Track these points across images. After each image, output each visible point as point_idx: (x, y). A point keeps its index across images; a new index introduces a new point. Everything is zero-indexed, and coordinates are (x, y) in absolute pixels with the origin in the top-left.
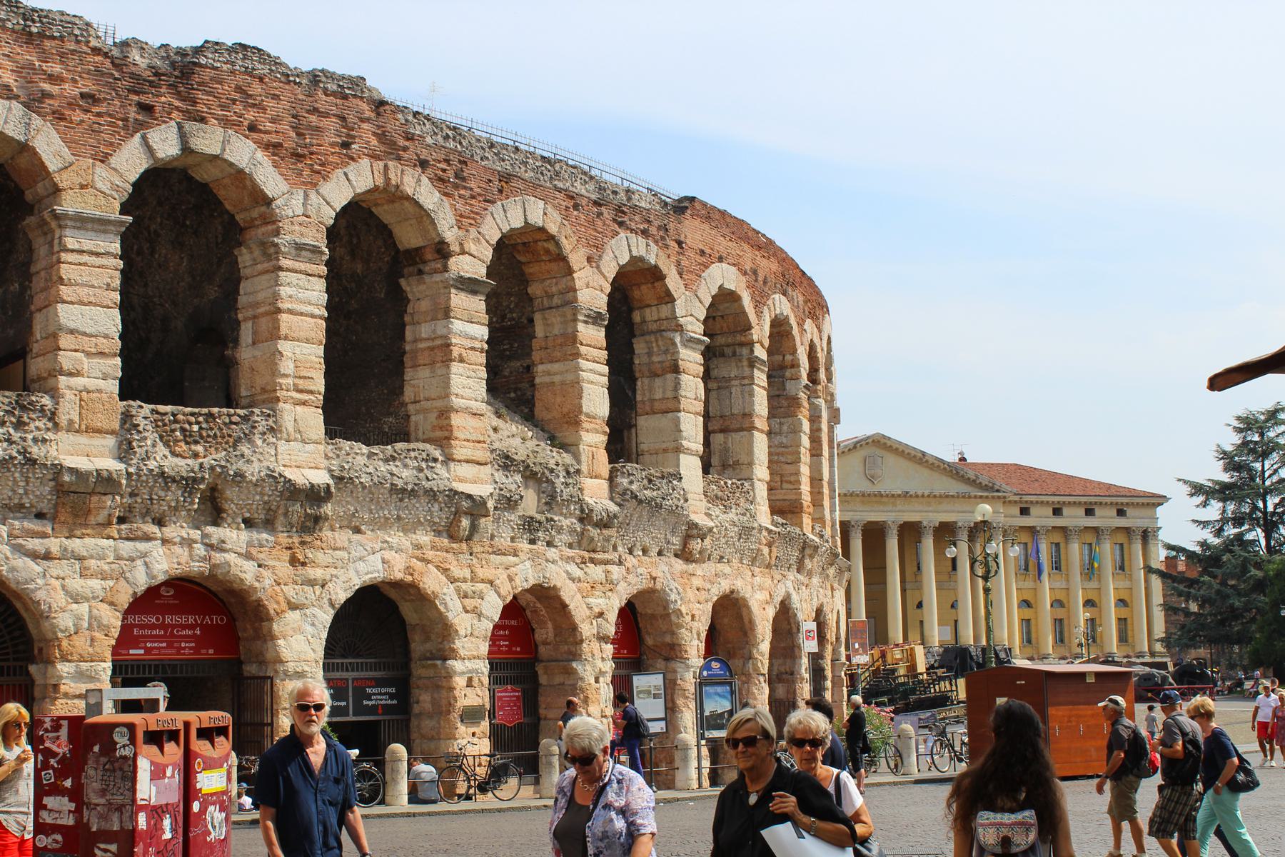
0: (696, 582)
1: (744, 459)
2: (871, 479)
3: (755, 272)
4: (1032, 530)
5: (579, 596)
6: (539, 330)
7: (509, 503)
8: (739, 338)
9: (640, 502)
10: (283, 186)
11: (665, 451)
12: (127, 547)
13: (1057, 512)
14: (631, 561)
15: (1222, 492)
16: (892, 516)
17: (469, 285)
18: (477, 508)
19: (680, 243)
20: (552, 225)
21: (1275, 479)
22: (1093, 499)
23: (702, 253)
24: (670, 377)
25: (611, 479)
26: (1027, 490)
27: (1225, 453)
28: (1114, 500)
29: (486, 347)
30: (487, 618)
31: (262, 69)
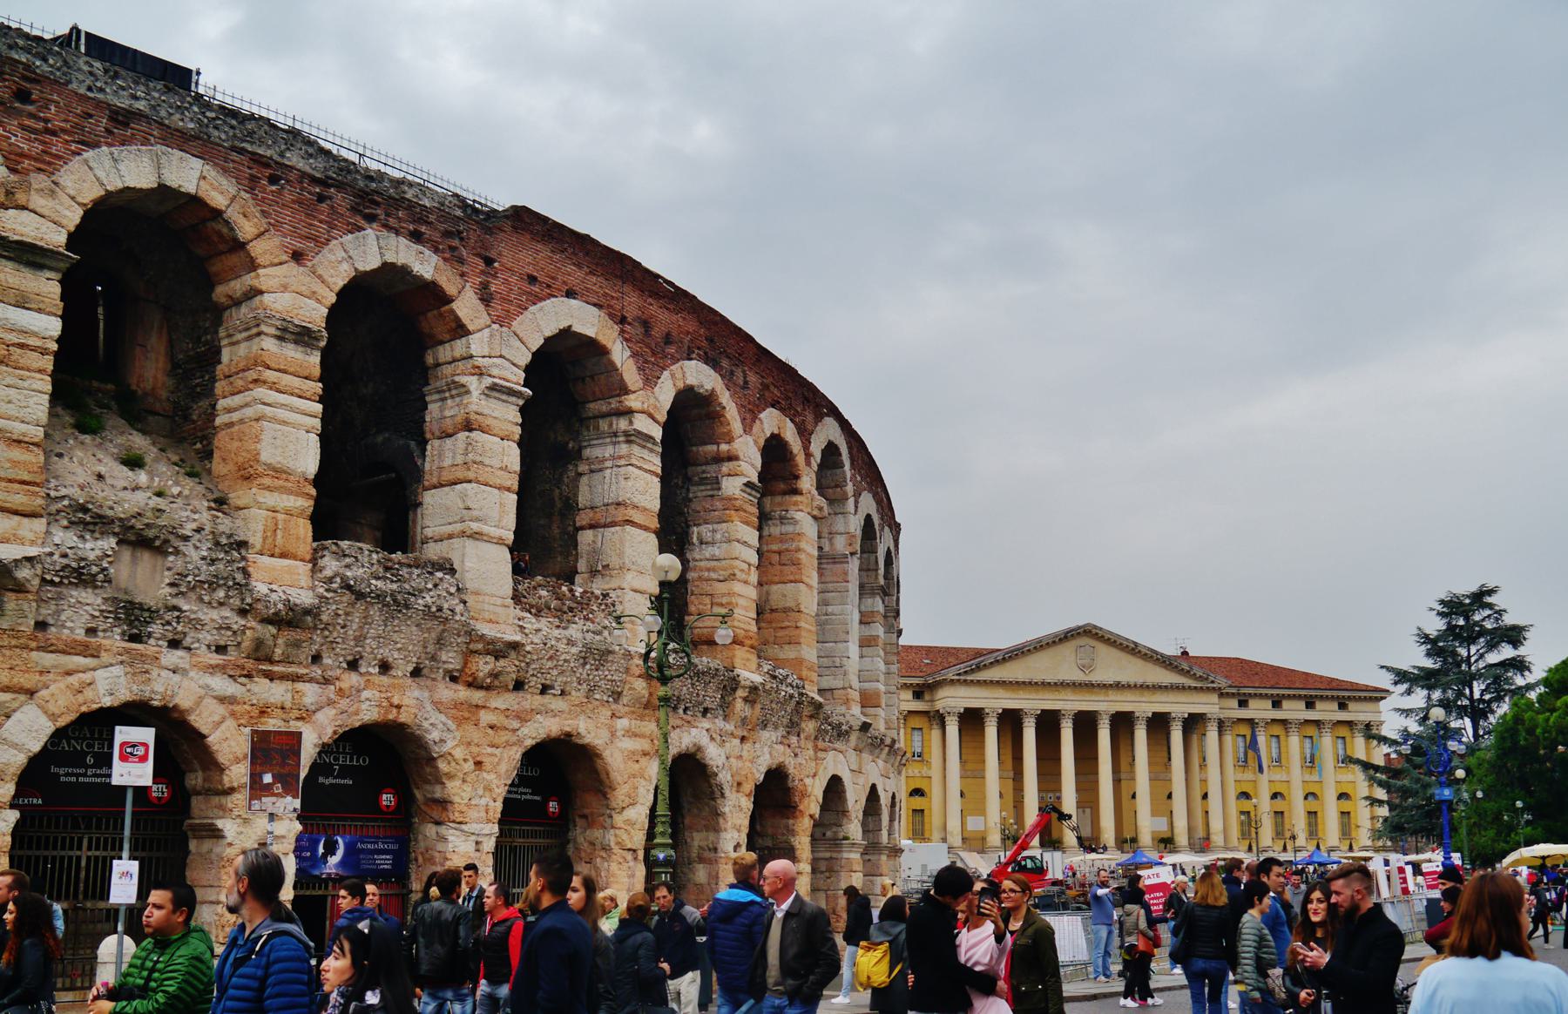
0: (486, 717)
1: (614, 561)
2: (1082, 668)
3: (646, 324)
4: (1251, 722)
5: (230, 723)
6: (226, 355)
7: (81, 575)
8: (614, 403)
9: (360, 596)
11: (450, 537)
13: (1277, 704)
14: (352, 679)
15: (1425, 679)
16: (1106, 705)
19: (489, 262)
20: (214, 194)
21: (1481, 664)
22: (1313, 693)
23: (532, 279)
24: (462, 435)
25: (314, 561)
26: (1246, 682)
27: (1426, 636)
28: (1335, 693)
29: (55, 347)
30: (15, 746)
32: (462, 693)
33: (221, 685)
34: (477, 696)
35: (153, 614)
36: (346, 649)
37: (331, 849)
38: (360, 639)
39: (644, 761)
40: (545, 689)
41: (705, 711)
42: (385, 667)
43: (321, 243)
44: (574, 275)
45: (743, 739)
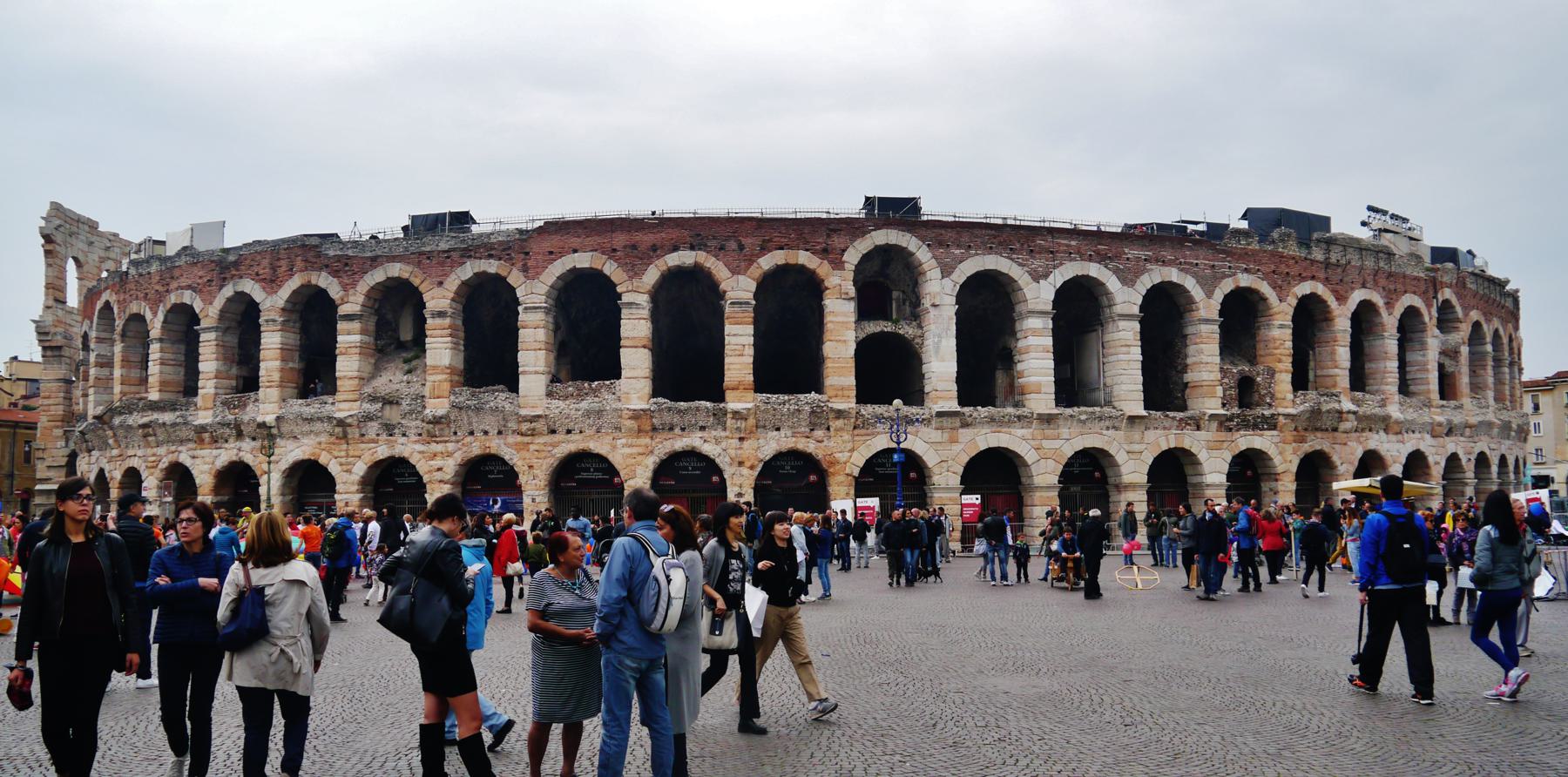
0: (532, 447)
7: (369, 418)
10: (263, 295)
12: (215, 452)
17: (349, 318)
18: (341, 423)
31: (259, 248)
32: (519, 439)
33: (419, 447)
34: (527, 439)
35: (394, 427)
36: (466, 428)
37: (495, 502)
38: (470, 424)
39: (639, 458)
40: (569, 432)
41: (703, 428)
42: (486, 433)
43: (446, 275)
44: (575, 242)
45: (741, 439)
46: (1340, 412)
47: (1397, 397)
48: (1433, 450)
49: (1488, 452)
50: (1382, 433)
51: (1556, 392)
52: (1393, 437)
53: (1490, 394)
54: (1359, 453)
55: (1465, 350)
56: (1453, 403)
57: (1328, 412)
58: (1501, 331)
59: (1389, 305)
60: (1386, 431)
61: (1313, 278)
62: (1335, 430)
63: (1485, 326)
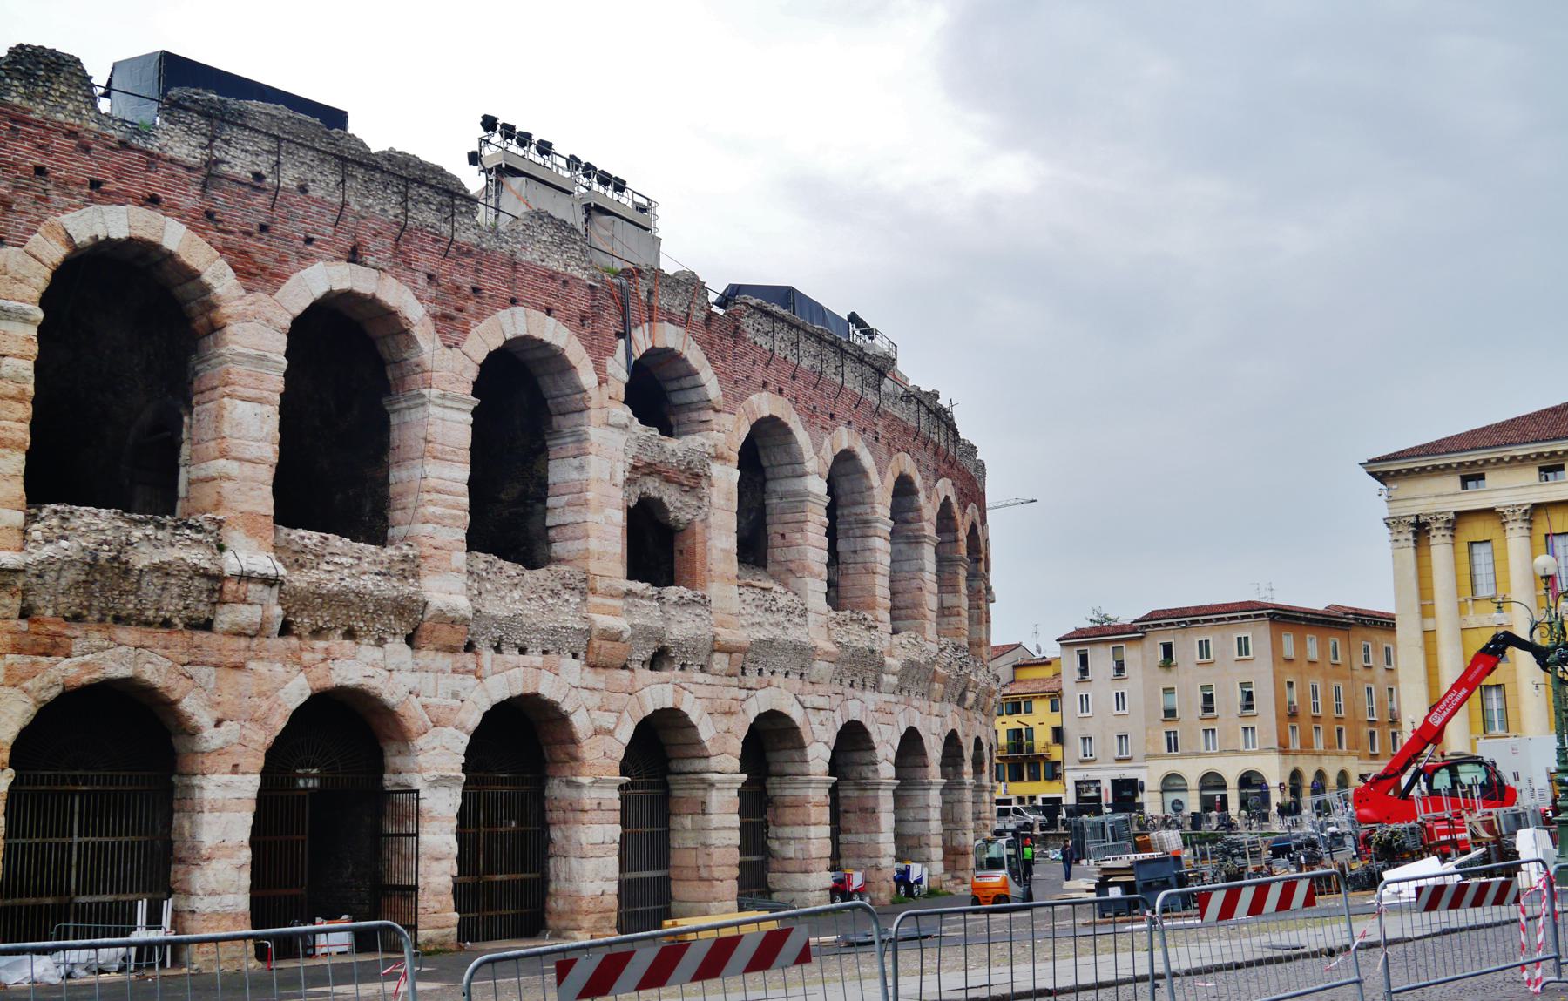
46: (216, 579)
47: (460, 557)
48: (594, 700)
49: (796, 714)
50: (397, 649)
51: (1146, 643)
52: (427, 657)
53: (815, 590)
54: (296, 691)
55: (726, 478)
56: (672, 592)
57: (162, 570)
58: (866, 459)
59: (449, 323)
60: (410, 640)
61: (153, 201)
62: (207, 625)
63: (802, 436)
